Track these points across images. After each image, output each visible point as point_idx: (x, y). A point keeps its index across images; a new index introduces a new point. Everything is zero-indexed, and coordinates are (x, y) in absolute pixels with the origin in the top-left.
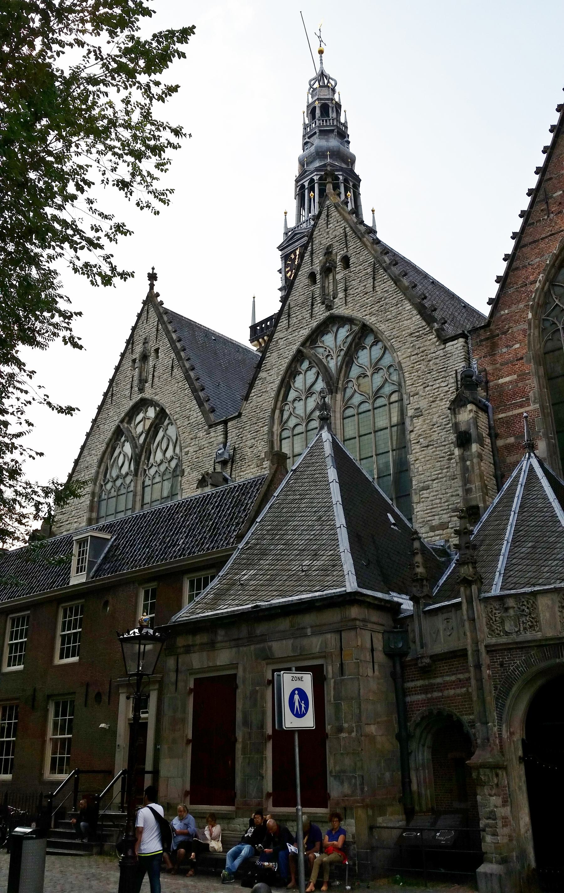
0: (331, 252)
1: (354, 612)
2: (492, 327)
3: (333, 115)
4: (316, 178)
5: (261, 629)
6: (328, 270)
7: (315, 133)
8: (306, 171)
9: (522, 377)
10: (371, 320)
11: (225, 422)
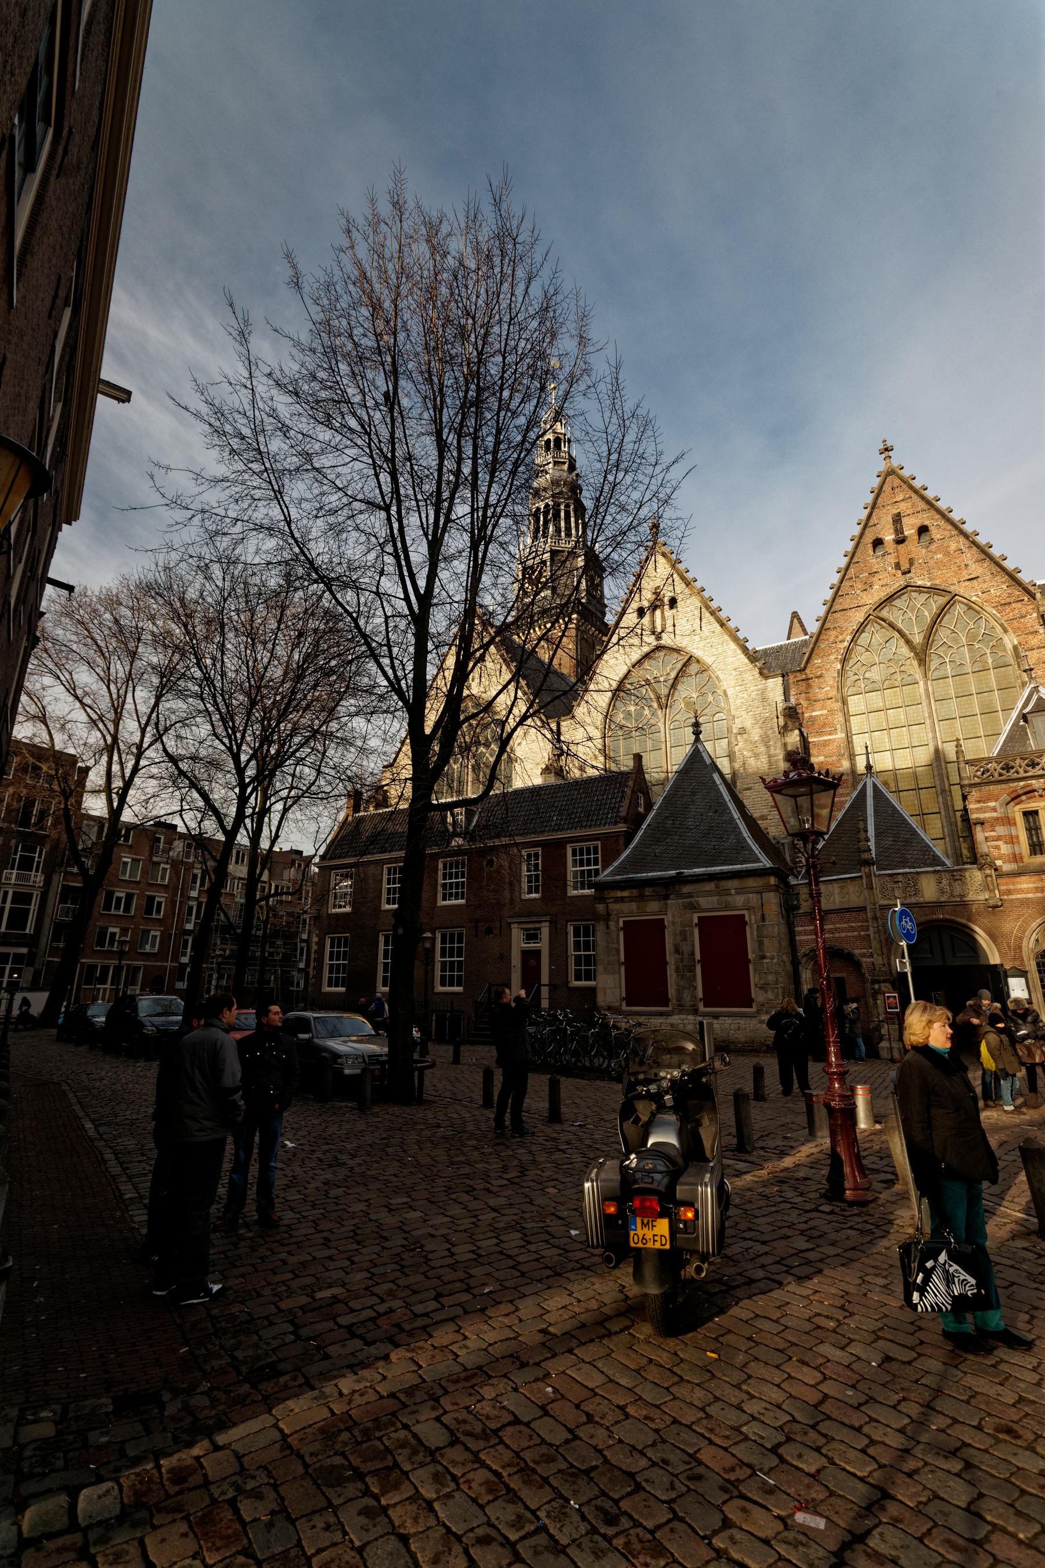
2: (808, 671)
6: (654, 607)
9: (831, 711)
10: (698, 653)
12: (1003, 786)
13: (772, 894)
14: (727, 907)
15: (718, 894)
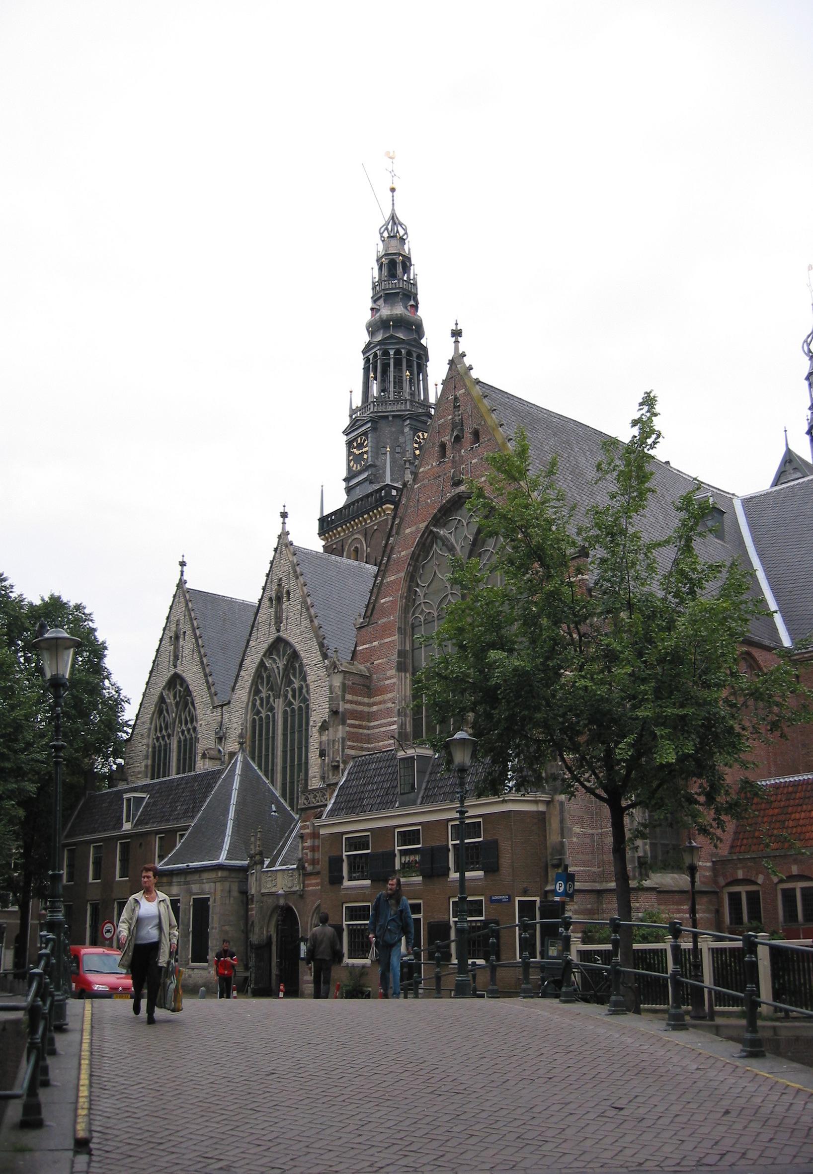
1: (220, 874)
3: (400, 270)
4: (378, 352)
5: (189, 878)
7: (381, 297)
8: (371, 343)
10: (298, 647)
11: (222, 706)
12: (313, 811)
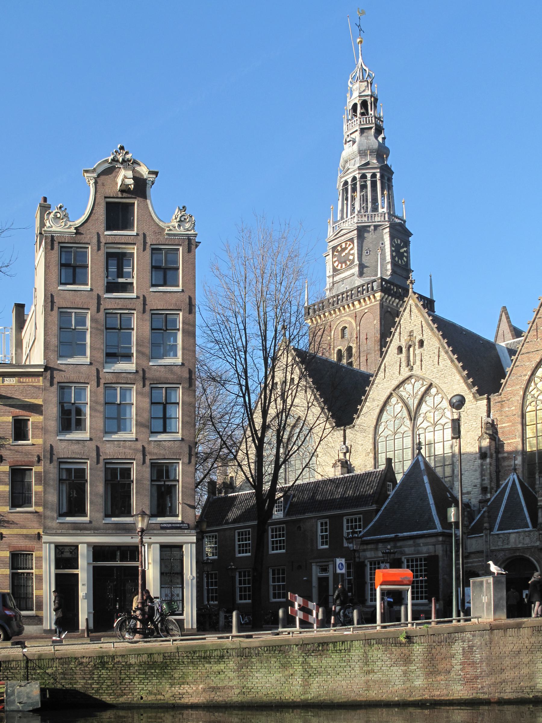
0: (412, 335)
7: (356, 131)
10: (436, 381)
13: (440, 546)
14: (418, 553)
15: (415, 546)
